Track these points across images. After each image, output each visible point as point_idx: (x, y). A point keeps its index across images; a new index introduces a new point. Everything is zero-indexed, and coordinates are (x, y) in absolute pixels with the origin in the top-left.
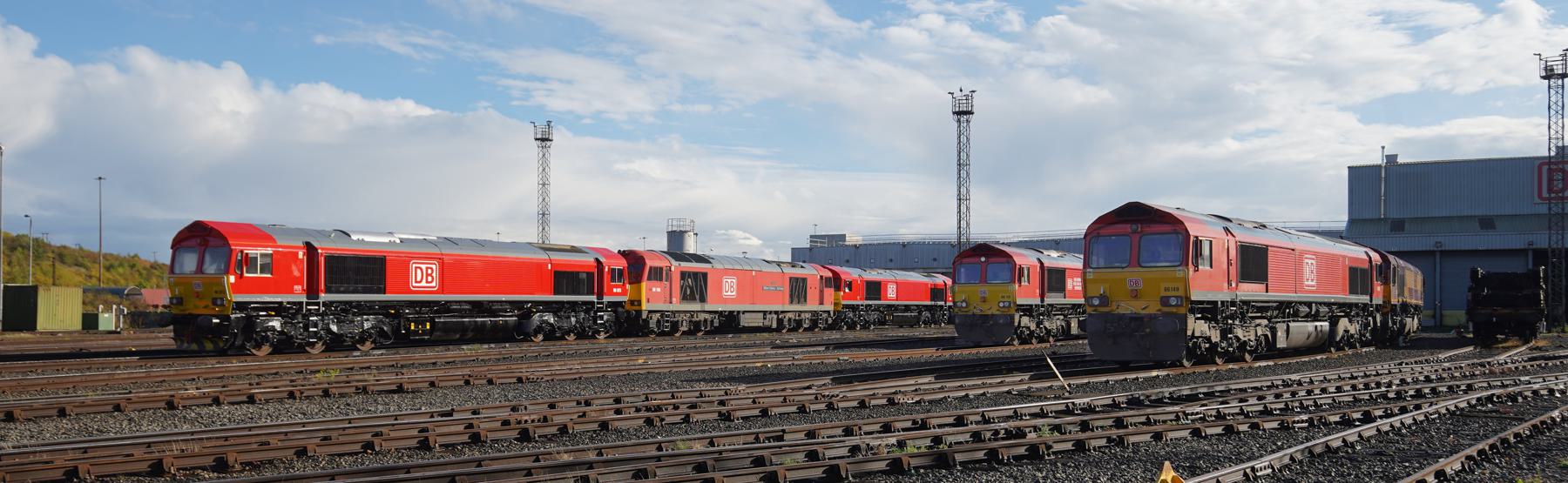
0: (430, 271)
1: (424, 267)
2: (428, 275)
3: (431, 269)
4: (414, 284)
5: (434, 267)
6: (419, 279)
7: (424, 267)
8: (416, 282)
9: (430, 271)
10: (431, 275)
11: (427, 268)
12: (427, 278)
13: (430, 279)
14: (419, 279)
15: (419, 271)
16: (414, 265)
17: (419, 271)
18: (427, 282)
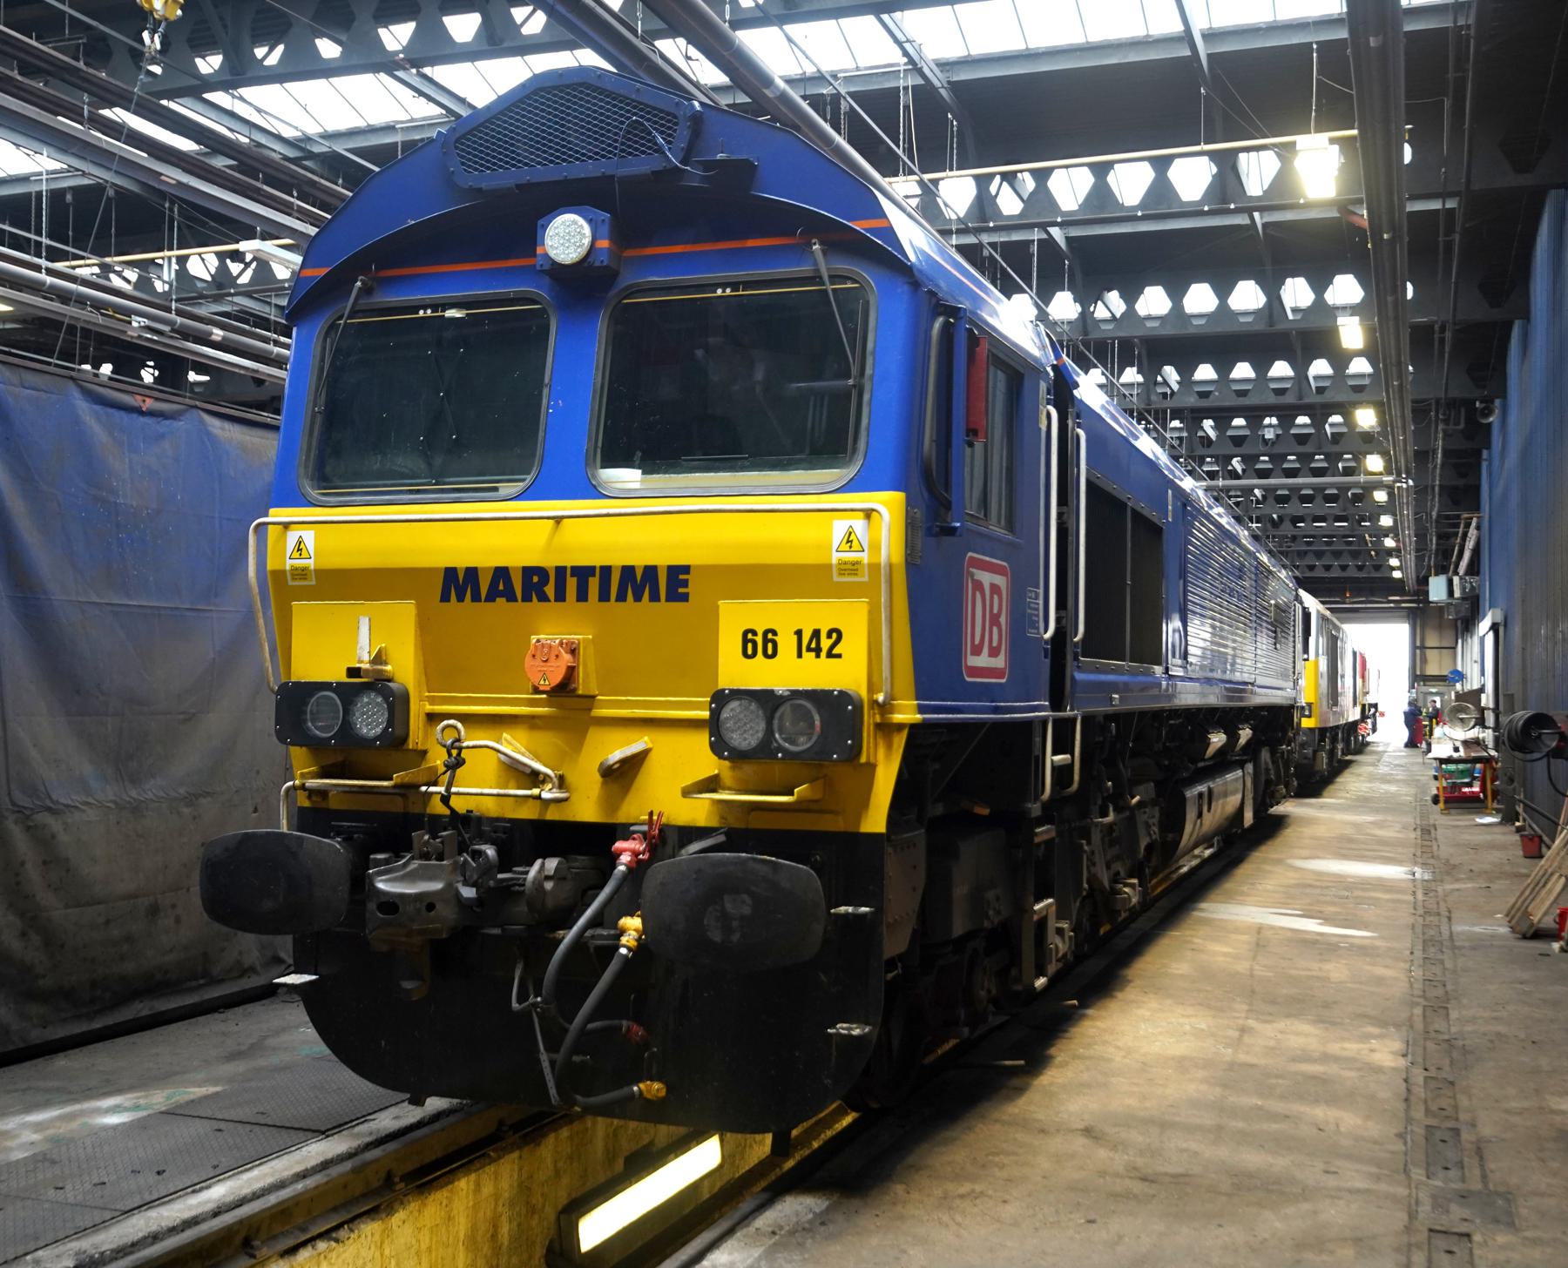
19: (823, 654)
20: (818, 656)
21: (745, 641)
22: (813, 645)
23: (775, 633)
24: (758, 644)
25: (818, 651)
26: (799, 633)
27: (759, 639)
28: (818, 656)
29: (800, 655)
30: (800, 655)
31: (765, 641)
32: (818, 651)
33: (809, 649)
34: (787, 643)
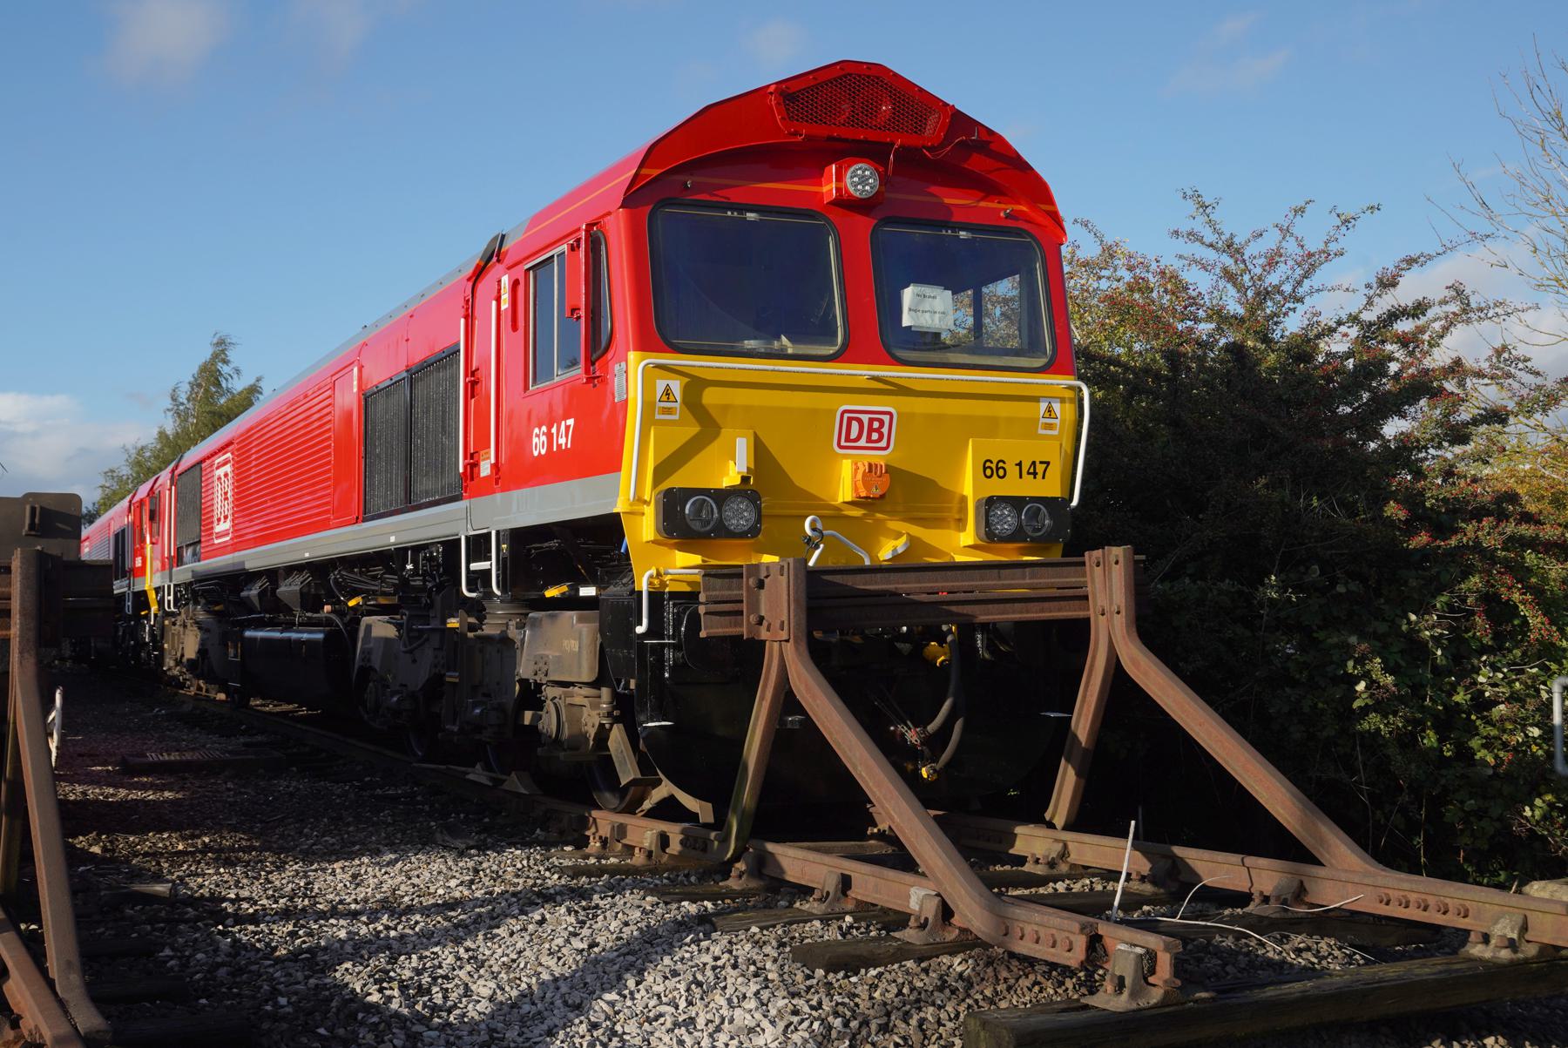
0: (876, 425)
1: (865, 418)
2: (871, 430)
3: (882, 422)
4: (843, 443)
5: (886, 418)
6: (854, 434)
7: (221, 472)
8: (847, 441)
9: (876, 425)
10: (878, 430)
11: (871, 421)
12: (869, 436)
13: (875, 436)
14: (854, 434)
15: (855, 425)
16: (846, 415)
17: (855, 425)
18: (869, 440)
19: (1040, 476)
20: (1035, 478)
21: (985, 468)
22: (1032, 470)
23: (1004, 463)
24: (993, 469)
25: (1035, 474)
26: (1019, 464)
27: (994, 466)
28: (1035, 478)
29: (1021, 477)
30: (1021, 477)
31: (998, 469)
32: (1035, 474)
33: (1029, 473)
34: (1012, 471)
